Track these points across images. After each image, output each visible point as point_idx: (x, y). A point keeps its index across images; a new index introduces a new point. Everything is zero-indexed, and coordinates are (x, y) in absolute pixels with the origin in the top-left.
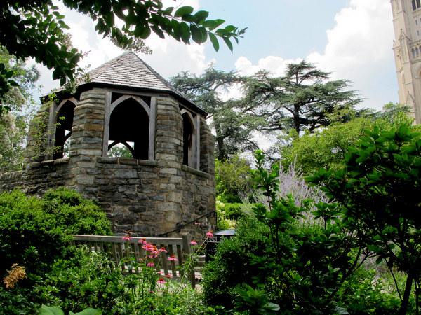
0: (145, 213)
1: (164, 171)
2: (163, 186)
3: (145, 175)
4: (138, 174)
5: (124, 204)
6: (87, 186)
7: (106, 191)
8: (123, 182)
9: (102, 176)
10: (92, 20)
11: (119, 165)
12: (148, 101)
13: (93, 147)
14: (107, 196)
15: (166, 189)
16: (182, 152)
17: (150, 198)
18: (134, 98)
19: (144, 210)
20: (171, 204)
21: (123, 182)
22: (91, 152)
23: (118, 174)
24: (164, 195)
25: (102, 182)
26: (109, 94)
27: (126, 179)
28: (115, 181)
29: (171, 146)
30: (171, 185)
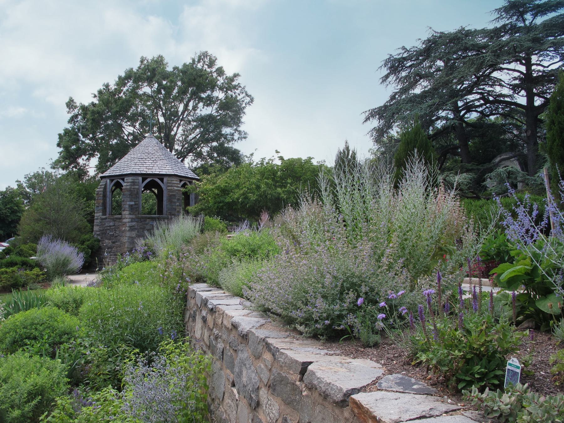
0: (117, 244)
1: (124, 221)
2: (123, 229)
3: (117, 224)
4: (114, 224)
5: (109, 240)
6: (97, 231)
7: (103, 233)
8: (109, 228)
9: (102, 226)
10: (225, 69)
11: (107, 220)
12: (123, 180)
13: (99, 212)
14: (103, 236)
15: (124, 230)
16: (183, 199)
17: (119, 235)
18: (119, 180)
19: (116, 242)
20: (127, 238)
21: (109, 228)
22: (98, 215)
23: (107, 224)
24: (124, 234)
25: (101, 229)
26: (108, 181)
27: (110, 226)
28: (106, 228)
29: (127, 206)
30: (127, 228)
